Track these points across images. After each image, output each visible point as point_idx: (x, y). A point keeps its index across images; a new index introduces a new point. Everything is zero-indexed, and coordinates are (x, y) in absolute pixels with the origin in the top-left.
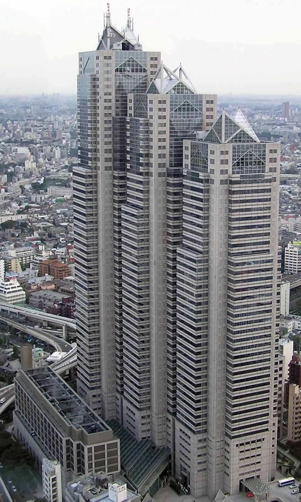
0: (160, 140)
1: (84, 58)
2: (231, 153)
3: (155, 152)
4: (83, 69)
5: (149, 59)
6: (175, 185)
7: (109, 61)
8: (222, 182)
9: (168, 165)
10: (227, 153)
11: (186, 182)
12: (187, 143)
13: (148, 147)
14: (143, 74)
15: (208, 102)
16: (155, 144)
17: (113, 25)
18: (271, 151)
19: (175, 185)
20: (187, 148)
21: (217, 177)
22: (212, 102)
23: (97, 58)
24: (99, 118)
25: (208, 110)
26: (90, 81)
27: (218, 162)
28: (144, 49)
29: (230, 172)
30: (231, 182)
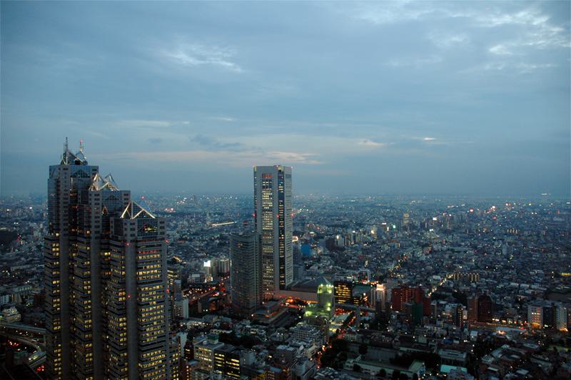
0: (96, 217)
1: (52, 169)
2: (136, 224)
3: (93, 224)
4: (51, 175)
5: (91, 171)
6: (105, 244)
7: (67, 171)
8: (131, 241)
9: (101, 231)
10: (134, 224)
11: (111, 242)
12: (112, 219)
13: (89, 222)
14: (88, 179)
15: (125, 195)
16: (93, 219)
17: (69, 148)
18: (161, 223)
19: (105, 244)
20: (112, 222)
21: (129, 238)
22: (127, 195)
23: (59, 169)
24: (60, 205)
25: (125, 199)
26: (56, 184)
27: (129, 229)
28: (89, 164)
29: (136, 235)
30: (137, 241)
